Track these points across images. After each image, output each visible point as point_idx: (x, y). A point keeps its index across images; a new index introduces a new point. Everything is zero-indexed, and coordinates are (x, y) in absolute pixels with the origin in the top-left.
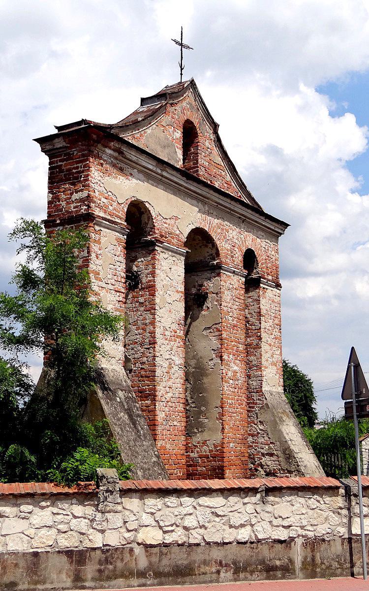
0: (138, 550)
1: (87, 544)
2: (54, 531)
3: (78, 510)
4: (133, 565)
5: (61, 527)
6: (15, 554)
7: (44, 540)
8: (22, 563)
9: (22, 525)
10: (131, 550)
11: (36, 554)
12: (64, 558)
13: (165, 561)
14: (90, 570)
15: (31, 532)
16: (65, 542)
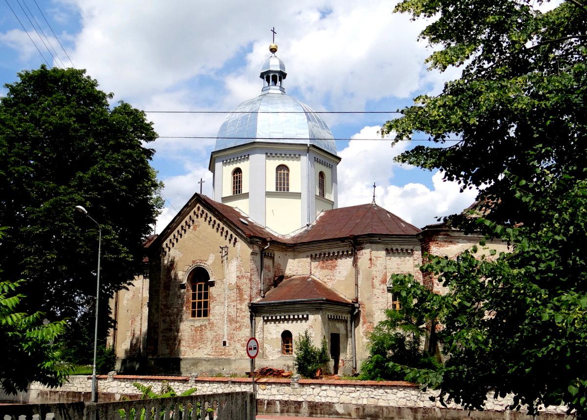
0: (437, 410)
1: (417, 406)
2: (405, 400)
3: (413, 392)
4: (435, 415)
5: (407, 398)
6: (392, 407)
7: (402, 403)
8: (395, 411)
9: (393, 397)
10: (434, 409)
11: (399, 408)
12: (410, 410)
13: (448, 415)
14: (419, 415)
15: (397, 399)
16: (409, 404)
